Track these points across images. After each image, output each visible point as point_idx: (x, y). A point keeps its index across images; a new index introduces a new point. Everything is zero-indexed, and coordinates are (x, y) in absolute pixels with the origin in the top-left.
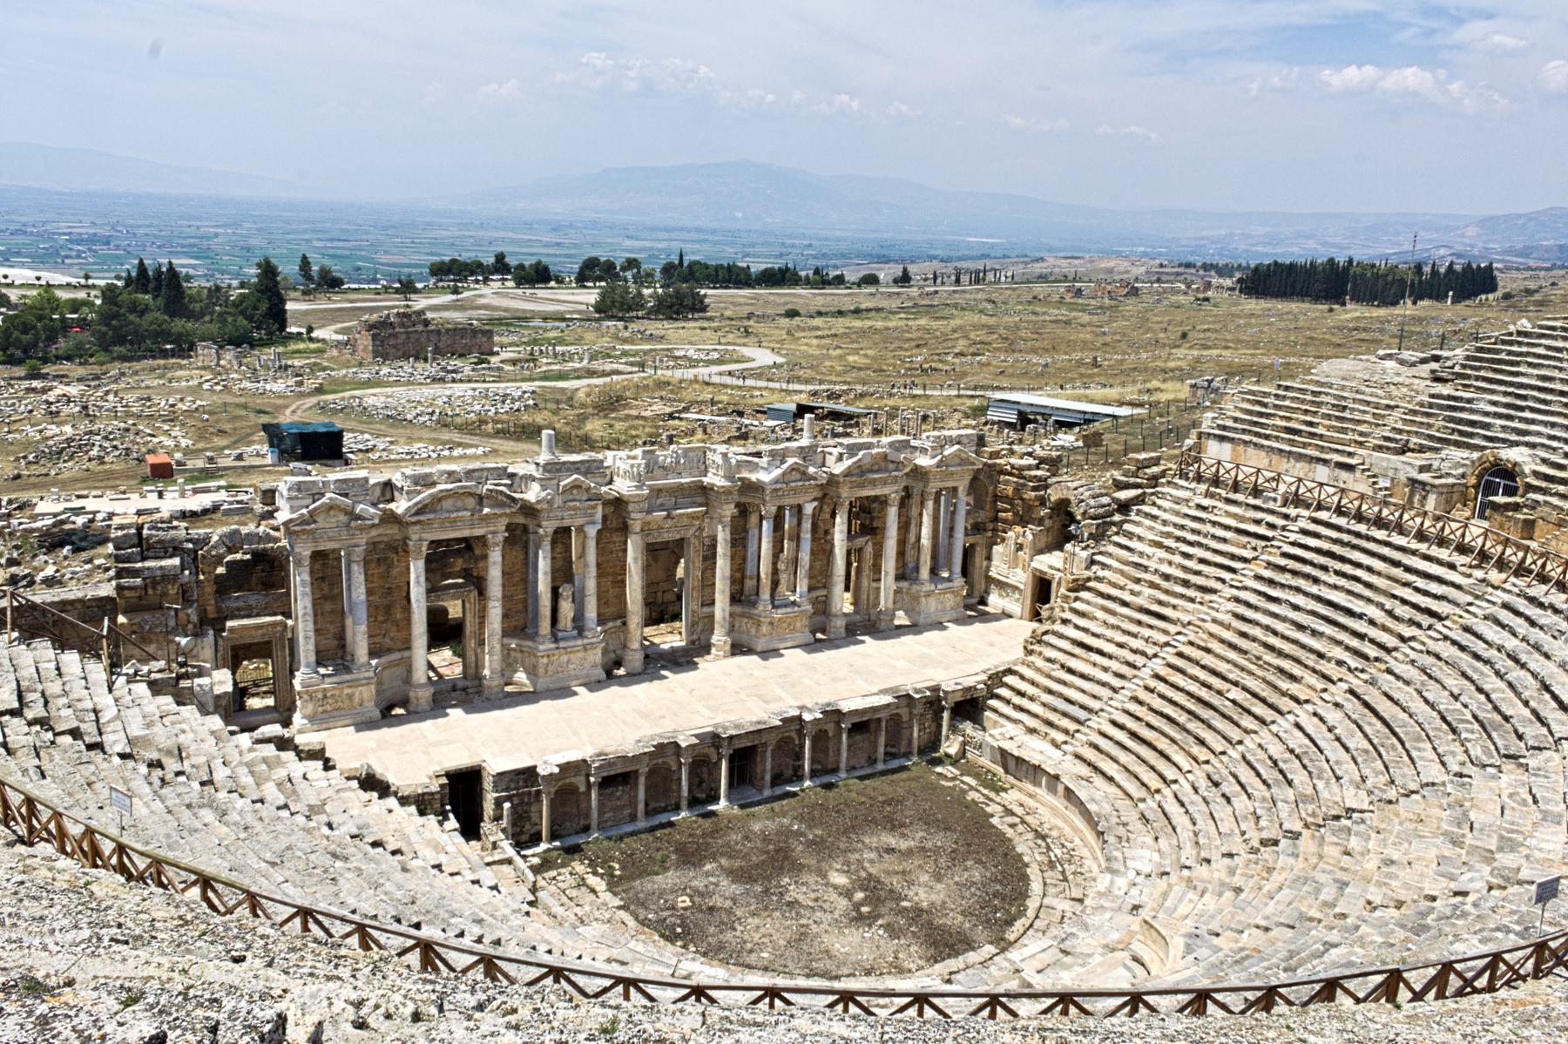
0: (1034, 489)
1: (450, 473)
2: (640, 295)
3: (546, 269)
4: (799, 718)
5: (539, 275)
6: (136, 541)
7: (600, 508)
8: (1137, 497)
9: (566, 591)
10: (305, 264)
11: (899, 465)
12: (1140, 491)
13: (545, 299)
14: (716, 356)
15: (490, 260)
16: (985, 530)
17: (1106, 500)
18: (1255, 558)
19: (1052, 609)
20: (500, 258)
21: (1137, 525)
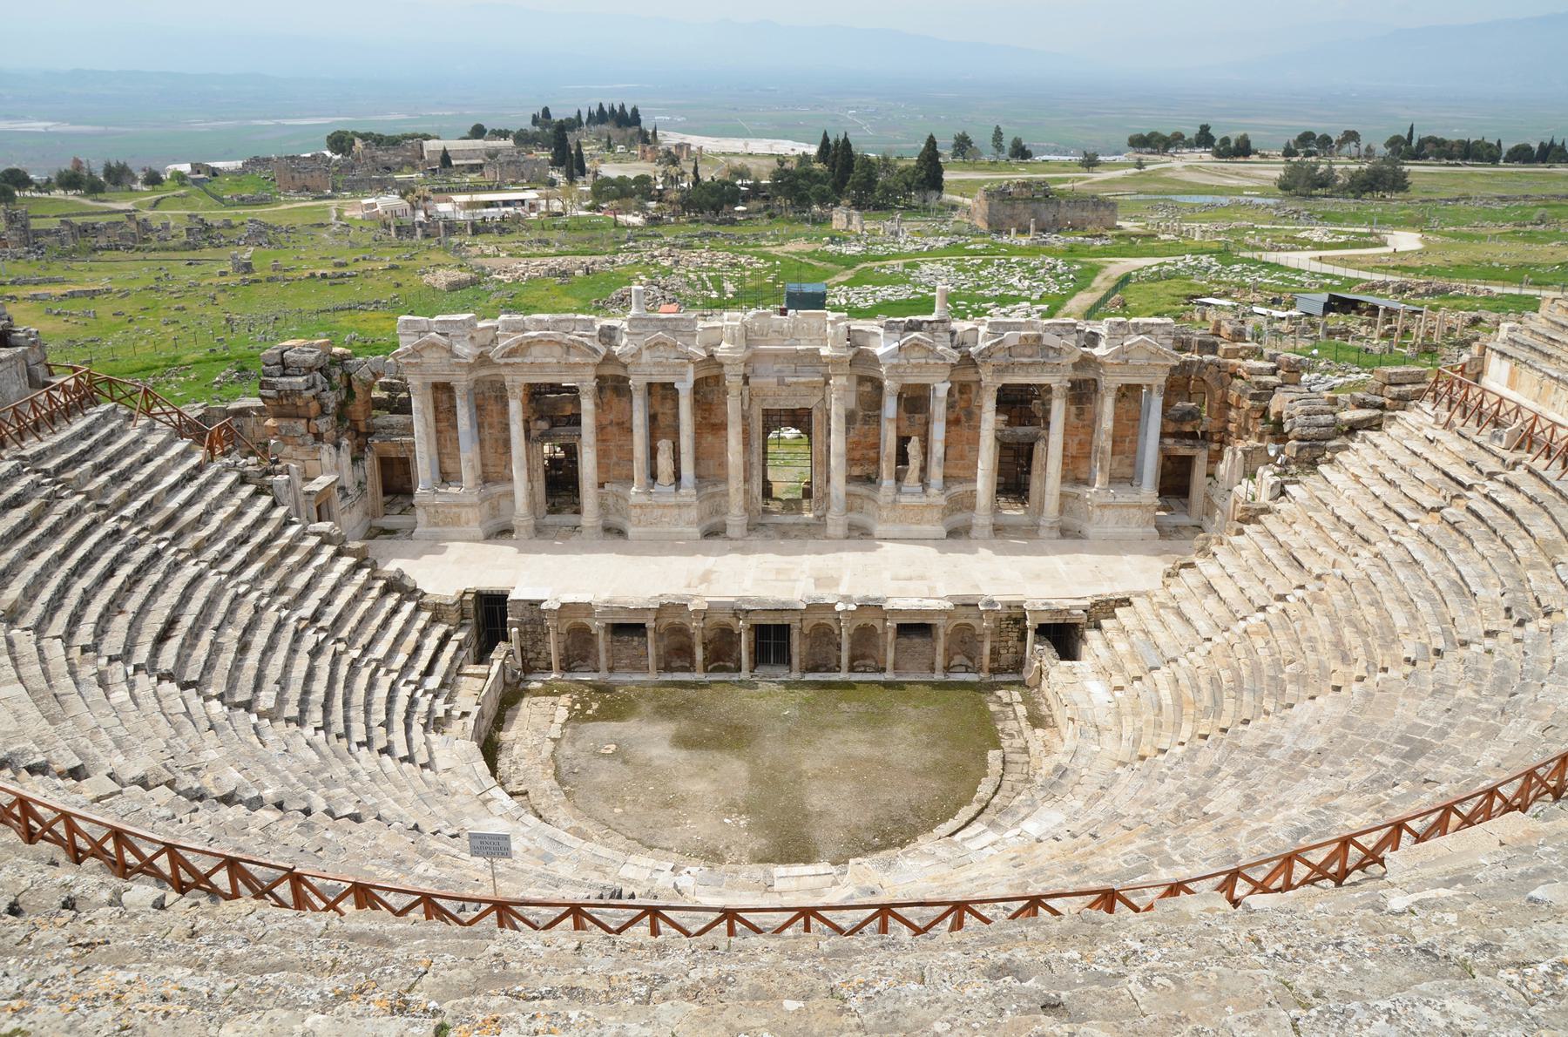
0: (1254, 397)
1: (539, 321)
2: (1331, 171)
3: (1248, 143)
4: (833, 606)
5: (1243, 149)
6: (278, 359)
7: (691, 367)
8: (1370, 419)
9: (664, 446)
10: (998, 135)
12: (1378, 412)
13: (1235, 174)
14: (1343, 238)
15: (1191, 132)
16: (1212, 441)
17: (1322, 419)
18: (1439, 509)
19: (1208, 539)
20: (1205, 129)
21: (1359, 455)
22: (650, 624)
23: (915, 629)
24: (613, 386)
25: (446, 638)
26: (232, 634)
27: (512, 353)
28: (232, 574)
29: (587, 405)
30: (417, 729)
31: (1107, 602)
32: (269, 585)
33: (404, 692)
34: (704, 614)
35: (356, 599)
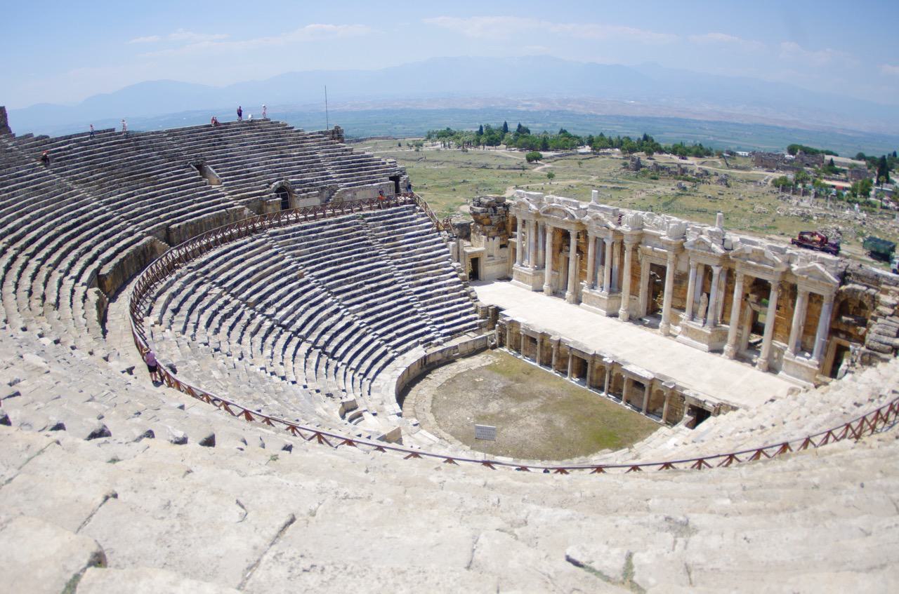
1: (558, 200)
4: (603, 357)
11: (774, 264)
22: (538, 340)
23: (638, 384)
24: (583, 233)
25: (476, 319)
26: (374, 285)
27: (547, 212)
28: (400, 269)
29: (573, 241)
30: (415, 341)
31: (728, 405)
32: (411, 276)
33: (427, 329)
34: (559, 343)
35: (446, 293)
